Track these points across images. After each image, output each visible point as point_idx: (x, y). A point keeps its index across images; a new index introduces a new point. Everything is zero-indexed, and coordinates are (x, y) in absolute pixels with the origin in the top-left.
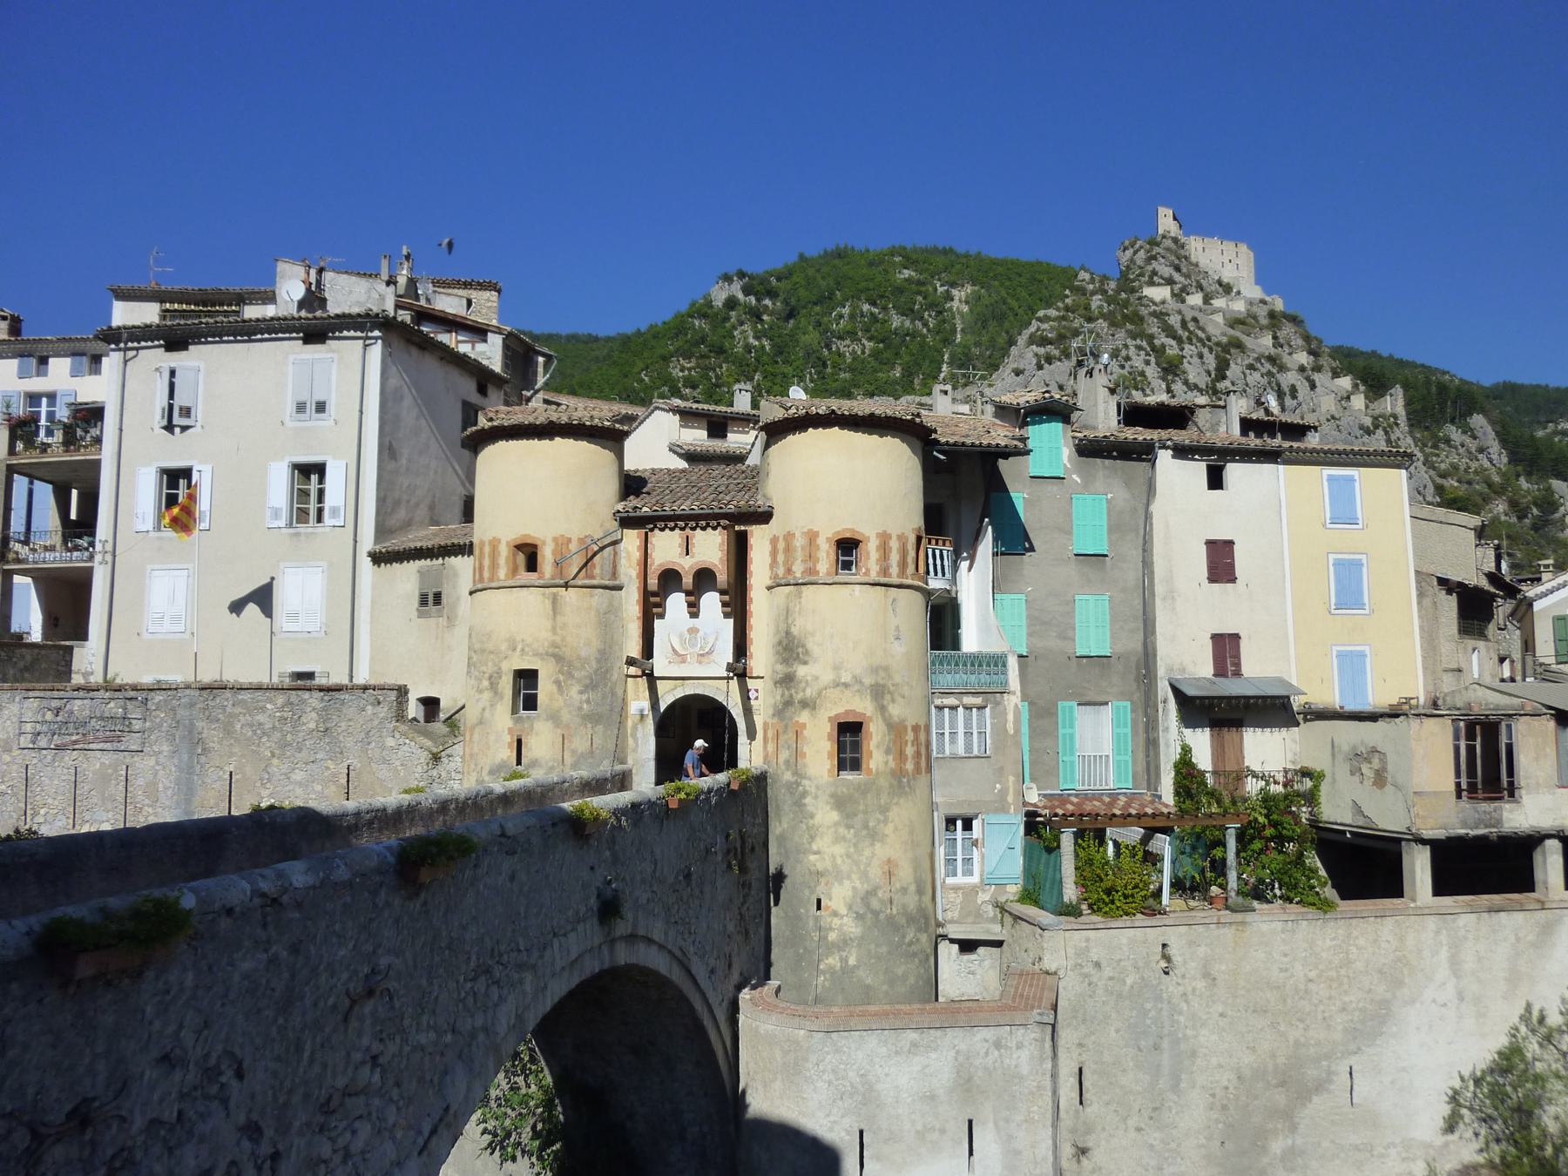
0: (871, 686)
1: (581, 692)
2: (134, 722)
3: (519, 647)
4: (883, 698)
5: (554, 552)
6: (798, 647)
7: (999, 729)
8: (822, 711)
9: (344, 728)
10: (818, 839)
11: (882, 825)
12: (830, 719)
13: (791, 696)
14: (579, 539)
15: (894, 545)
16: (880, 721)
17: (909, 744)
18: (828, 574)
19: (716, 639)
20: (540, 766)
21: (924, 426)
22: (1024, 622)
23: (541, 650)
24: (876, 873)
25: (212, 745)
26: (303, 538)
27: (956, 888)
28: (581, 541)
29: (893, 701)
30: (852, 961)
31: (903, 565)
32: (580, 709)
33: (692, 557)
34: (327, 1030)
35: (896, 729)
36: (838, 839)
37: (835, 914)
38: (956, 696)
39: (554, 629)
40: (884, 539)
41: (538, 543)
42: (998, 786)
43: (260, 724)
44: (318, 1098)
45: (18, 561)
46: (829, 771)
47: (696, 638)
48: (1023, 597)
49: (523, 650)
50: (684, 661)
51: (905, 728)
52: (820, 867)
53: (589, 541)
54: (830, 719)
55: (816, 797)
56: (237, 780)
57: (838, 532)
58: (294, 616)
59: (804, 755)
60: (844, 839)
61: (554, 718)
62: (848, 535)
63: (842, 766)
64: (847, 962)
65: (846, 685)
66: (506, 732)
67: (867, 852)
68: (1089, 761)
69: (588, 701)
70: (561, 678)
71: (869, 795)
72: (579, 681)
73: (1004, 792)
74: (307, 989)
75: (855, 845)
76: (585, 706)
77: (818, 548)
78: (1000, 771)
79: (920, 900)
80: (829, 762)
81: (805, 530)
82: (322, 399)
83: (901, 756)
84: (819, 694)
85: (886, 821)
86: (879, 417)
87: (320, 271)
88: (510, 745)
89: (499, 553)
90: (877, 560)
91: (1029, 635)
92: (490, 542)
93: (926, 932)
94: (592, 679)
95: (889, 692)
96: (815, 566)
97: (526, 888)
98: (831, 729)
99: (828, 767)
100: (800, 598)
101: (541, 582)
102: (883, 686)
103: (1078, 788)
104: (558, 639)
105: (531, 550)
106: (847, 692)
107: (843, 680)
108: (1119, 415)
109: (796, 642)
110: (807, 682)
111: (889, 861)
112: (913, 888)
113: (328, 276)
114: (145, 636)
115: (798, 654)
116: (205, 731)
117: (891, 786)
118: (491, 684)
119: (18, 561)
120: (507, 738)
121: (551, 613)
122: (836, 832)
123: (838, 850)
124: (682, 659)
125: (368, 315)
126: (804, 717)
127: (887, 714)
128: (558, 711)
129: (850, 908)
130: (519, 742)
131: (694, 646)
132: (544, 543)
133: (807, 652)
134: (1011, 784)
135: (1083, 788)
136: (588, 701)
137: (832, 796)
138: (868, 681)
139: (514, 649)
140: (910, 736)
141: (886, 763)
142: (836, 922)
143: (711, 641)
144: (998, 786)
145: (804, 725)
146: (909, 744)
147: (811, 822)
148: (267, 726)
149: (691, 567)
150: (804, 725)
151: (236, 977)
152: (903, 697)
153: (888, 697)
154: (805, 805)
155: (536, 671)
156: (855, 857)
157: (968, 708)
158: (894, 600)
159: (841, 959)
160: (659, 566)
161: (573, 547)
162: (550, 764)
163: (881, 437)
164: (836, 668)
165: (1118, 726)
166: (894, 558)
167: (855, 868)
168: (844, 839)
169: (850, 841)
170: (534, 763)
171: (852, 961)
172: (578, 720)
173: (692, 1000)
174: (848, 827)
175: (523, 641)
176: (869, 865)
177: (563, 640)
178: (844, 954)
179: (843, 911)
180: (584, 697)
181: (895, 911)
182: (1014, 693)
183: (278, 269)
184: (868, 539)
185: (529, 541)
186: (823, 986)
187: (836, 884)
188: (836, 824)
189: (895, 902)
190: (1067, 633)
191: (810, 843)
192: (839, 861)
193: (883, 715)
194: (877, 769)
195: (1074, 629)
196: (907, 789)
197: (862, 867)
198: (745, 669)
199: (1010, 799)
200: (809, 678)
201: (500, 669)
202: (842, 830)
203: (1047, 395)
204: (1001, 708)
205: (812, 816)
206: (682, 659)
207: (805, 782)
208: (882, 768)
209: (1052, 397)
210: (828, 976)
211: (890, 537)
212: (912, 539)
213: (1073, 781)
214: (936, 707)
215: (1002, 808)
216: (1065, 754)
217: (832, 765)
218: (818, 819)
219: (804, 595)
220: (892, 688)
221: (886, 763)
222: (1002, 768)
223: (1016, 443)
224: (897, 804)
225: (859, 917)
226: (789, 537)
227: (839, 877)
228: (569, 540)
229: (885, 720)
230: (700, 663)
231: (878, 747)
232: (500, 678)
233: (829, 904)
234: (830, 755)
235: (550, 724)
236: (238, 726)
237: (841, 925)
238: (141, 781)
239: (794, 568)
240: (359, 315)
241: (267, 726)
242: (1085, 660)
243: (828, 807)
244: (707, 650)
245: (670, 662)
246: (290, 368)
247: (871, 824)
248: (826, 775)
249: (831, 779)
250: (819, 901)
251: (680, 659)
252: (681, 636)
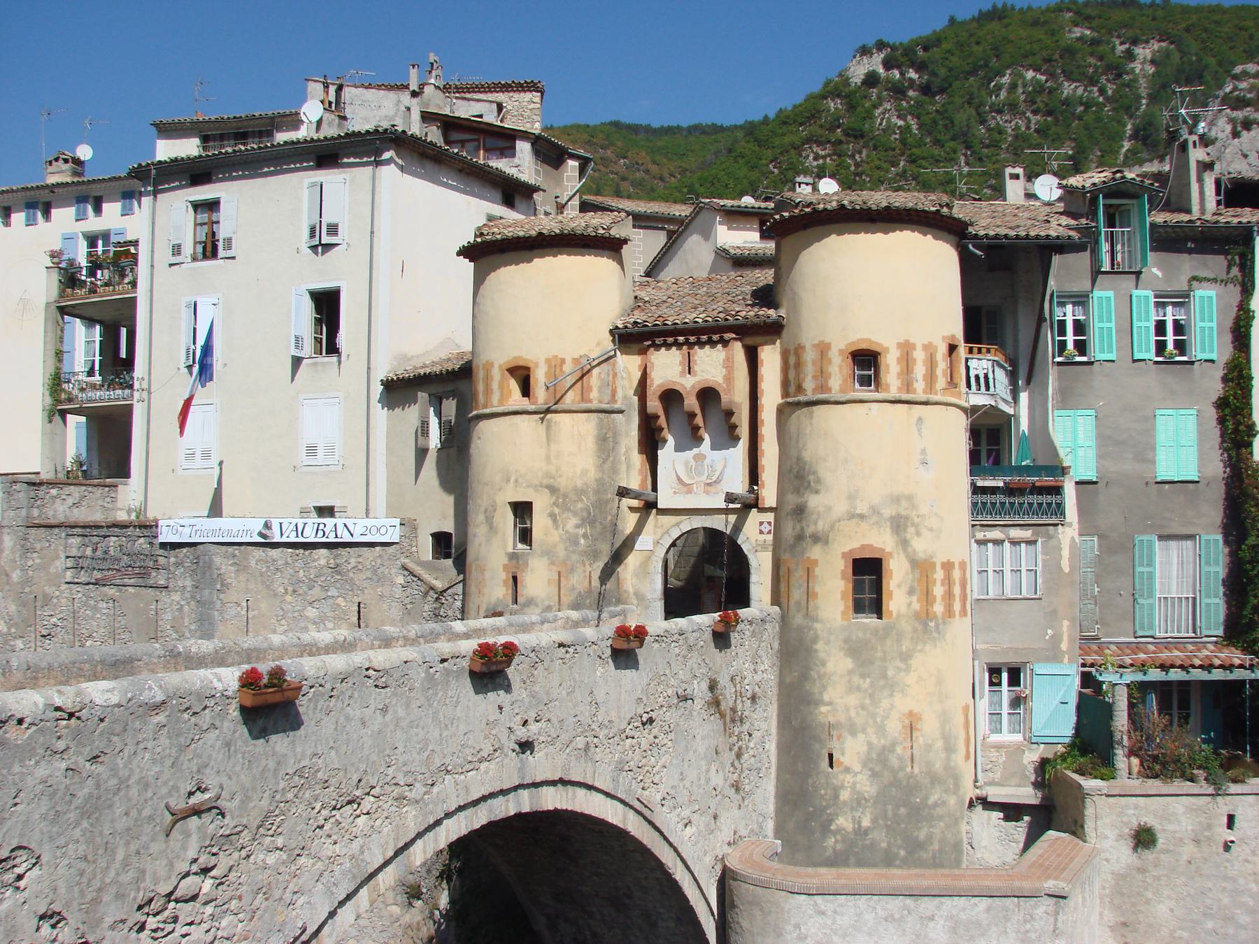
0: (892, 517)
1: (577, 526)
2: (160, 559)
3: (512, 480)
4: (905, 530)
5: (547, 375)
6: (809, 474)
7: (1053, 567)
8: (836, 545)
9: (353, 564)
10: (830, 689)
11: (902, 674)
12: (844, 555)
13: (802, 529)
14: (573, 359)
15: (919, 355)
16: (902, 556)
17: (938, 583)
18: (842, 391)
19: (725, 467)
20: (537, 605)
21: (955, 218)
22: (1093, 444)
23: (536, 482)
24: (894, 727)
25: (229, 581)
26: (319, 368)
27: (998, 747)
28: (576, 361)
29: (918, 534)
30: (866, 822)
31: (931, 378)
32: (576, 543)
33: (695, 375)
34: (144, 838)
35: (922, 568)
36: (851, 689)
37: (847, 770)
38: (1000, 528)
39: (548, 459)
40: (907, 350)
41: (531, 365)
42: (1049, 631)
43: (274, 561)
44: (135, 899)
45: (70, 400)
46: (843, 613)
47: (702, 466)
48: (1092, 412)
49: (516, 481)
50: (690, 492)
51: (933, 565)
52: (831, 719)
53: (584, 361)
54: (844, 555)
55: (827, 643)
56: (254, 617)
57: (853, 343)
58: (312, 450)
59: (815, 595)
60: (859, 688)
61: (548, 553)
62: (864, 346)
63: (859, 607)
64: (859, 823)
65: (862, 517)
66: (501, 568)
67: (885, 703)
68: (1173, 604)
69: (585, 536)
70: (556, 510)
71: (888, 642)
72: (575, 514)
73: (1056, 639)
74: (116, 798)
75: (871, 696)
76: (582, 541)
77: (830, 362)
78: (1053, 615)
79: (948, 759)
80: (843, 602)
81: (816, 342)
82: (333, 221)
83: (928, 597)
84: (832, 527)
85: (908, 669)
86: (898, 210)
87: (340, 88)
88: (505, 582)
89: (492, 377)
90: (899, 374)
91: (1100, 457)
93: (955, 793)
94: (590, 513)
95: (913, 524)
96: (826, 381)
97: (404, 724)
98: (846, 567)
99: (842, 608)
100: (811, 418)
101: (532, 408)
102: (907, 518)
103: (1158, 635)
104: (552, 469)
105: (525, 373)
106: (864, 525)
107: (858, 511)
108: (1218, 193)
109: (807, 468)
110: (819, 514)
111: (911, 714)
112: (939, 744)
113: (348, 93)
114: (180, 471)
115: (809, 484)
116: (224, 567)
117: (915, 631)
118: (487, 517)
119: (70, 400)
120: (503, 576)
121: (544, 440)
122: (850, 681)
123: (852, 700)
124: (686, 487)
125: (376, 131)
126: (815, 552)
127: (910, 549)
128: (555, 546)
129: (865, 765)
130: (515, 579)
131: (700, 474)
132: (537, 365)
133: (818, 481)
134: (1065, 629)
135: (1163, 635)
136: (585, 536)
137: (846, 641)
138: (888, 512)
139: (508, 481)
140: (939, 574)
141: (910, 604)
142: (849, 778)
143: (719, 468)
144: (1049, 631)
145: (816, 562)
146: (938, 583)
147: (823, 670)
148: (280, 562)
149: (693, 386)
150: (816, 562)
151: (30, 782)
152: (931, 530)
153: (911, 530)
154: (816, 651)
155: (531, 503)
156: (871, 709)
157: (1015, 543)
158: (920, 419)
159: (854, 819)
160: (659, 386)
161: (568, 368)
162: (547, 603)
163: (886, 232)
164: (852, 497)
165: (1208, 563)
166: (920, 370)
167: (870, 721)
168: (859, 688)
169: (866, 691)
170: (530, 602)
171: (866, 822)
172: (575, 557)
173: (657, 853)
174: (863, 676)
175: (516, 471)
176: (885, 718)
177: (558, 469)
178: (858, 814)
179: (857, 767)
180: (581, 531)
181: (916, 770)
182: (1070, 525)
183: (309, 89)
184: (887, 350)
185: (521, 363)
186: (834, 850)
187: (849, 737)
188: (850, 672)
189: (916, 759)
190: (1145, 451)
191: (821, 693)
192: (853, 713)
193: (905, 550)
194: (899, 615)
195: (1153, 449)
196: (934, 634)
197: (879, 720)
198: (757, 499)
199: (1064, 646)
200: (821, 509)
201: (494, 502)
202: (856, 679)
203: (1118, 175)
204: (1053, 542)
205: (824, 663)
206: (686, 487)
207: (817, 626)
208: (903, 610)
209: (1123, 177)
210: (839, 837)
211: (913, 347)
212: (942, 349)
213: (1151, 627)
214: (976, 541)
215: (1055, 657)
216: (1142, 596)
217: (846, 607)
218: (830, 667)
219: (815, 415)
220: (916, 520)
221: (910, 604)
222: (1054, 613)
223: (1072, 233)
224: (920, 651)
225: (874, 775)
226: (799, 350)
227: (853, 730)
228: (563, 361)
229: (907, 557)
230: (707, 493)
231: (899, 586)
232: (495, 510)
233: (842, 759)
234: (843, 597)
235: (545, 561)
236: (253, 563)
237: (854, 784)
238: (168, 616)
240: (368, 132)
241: (280, 562)
242: (1167, 486)
243: (841, 654)
244: (714, 478)
245: (675, 493)
246: (306, 192)
247: (890, 673)
248: (839, 617)
249: (845, 623)
250: (831, 756)
251: (685, 489)
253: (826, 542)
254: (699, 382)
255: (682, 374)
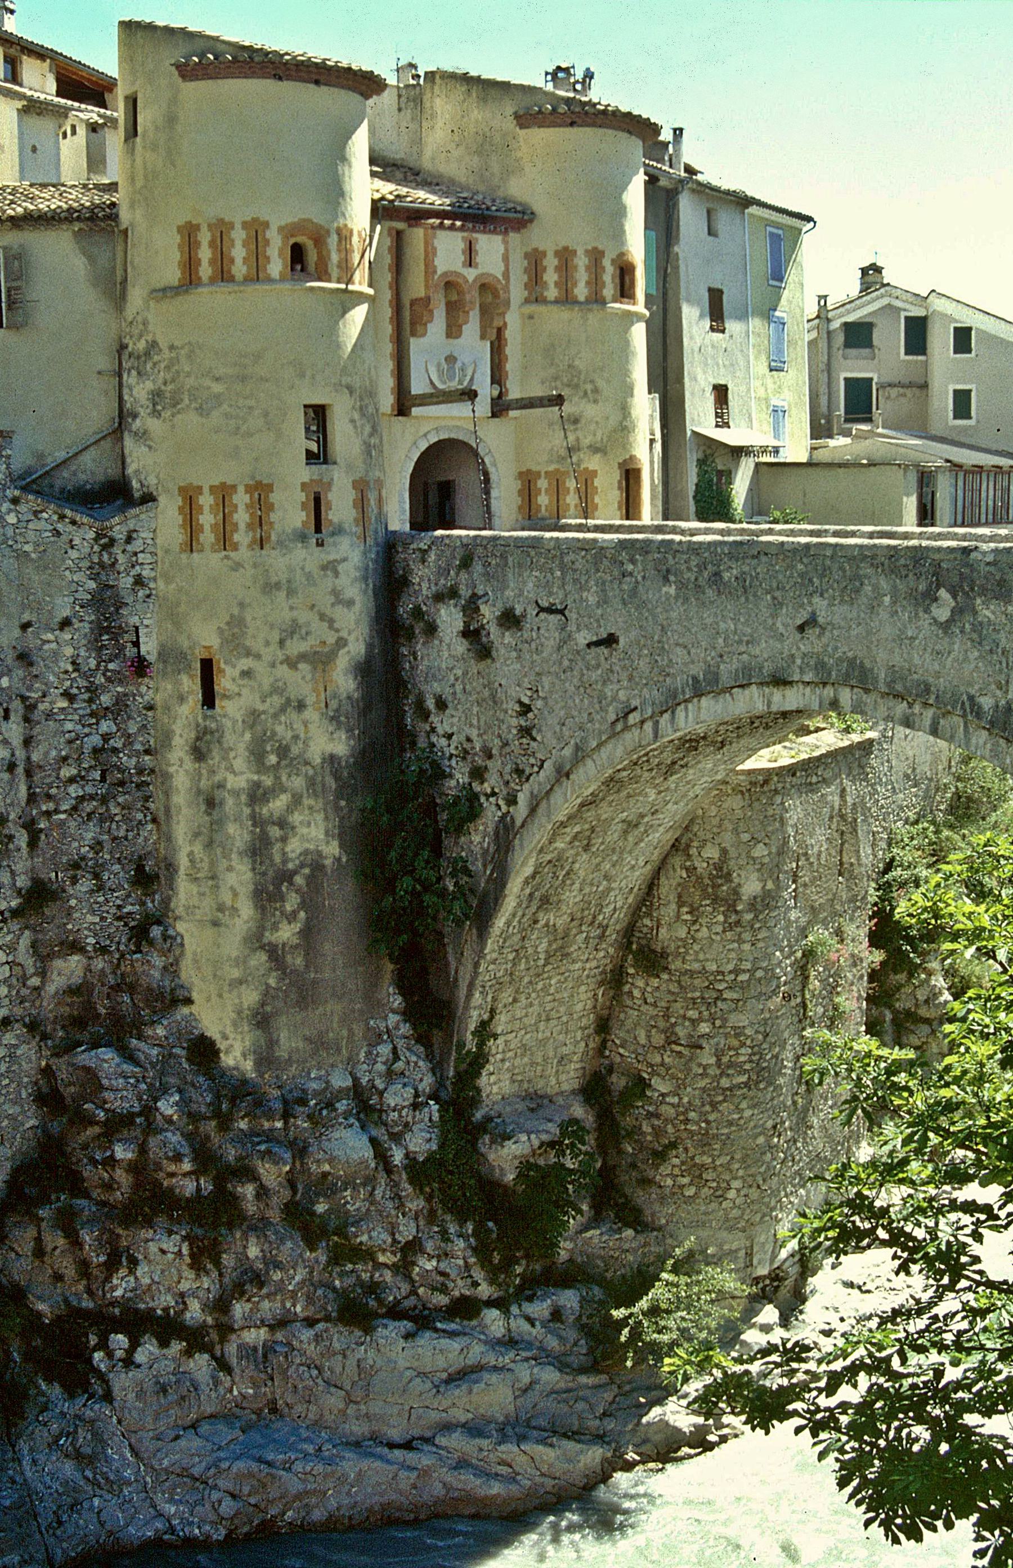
13: (578, 439)
33: (476, 267)
47: (453, 368)
49: (313, 377)
77: (603, 269)
88: (304, 506)
92: (245, 225)
120: (303, 496)
130: (317, 500)
143: (470, 373)
145: (595, 473)
150: (595, 473)
239: (576, 291)
252: (439, 365)
253: (606, 454)
254: (483, 274)
255: (464, 265)
